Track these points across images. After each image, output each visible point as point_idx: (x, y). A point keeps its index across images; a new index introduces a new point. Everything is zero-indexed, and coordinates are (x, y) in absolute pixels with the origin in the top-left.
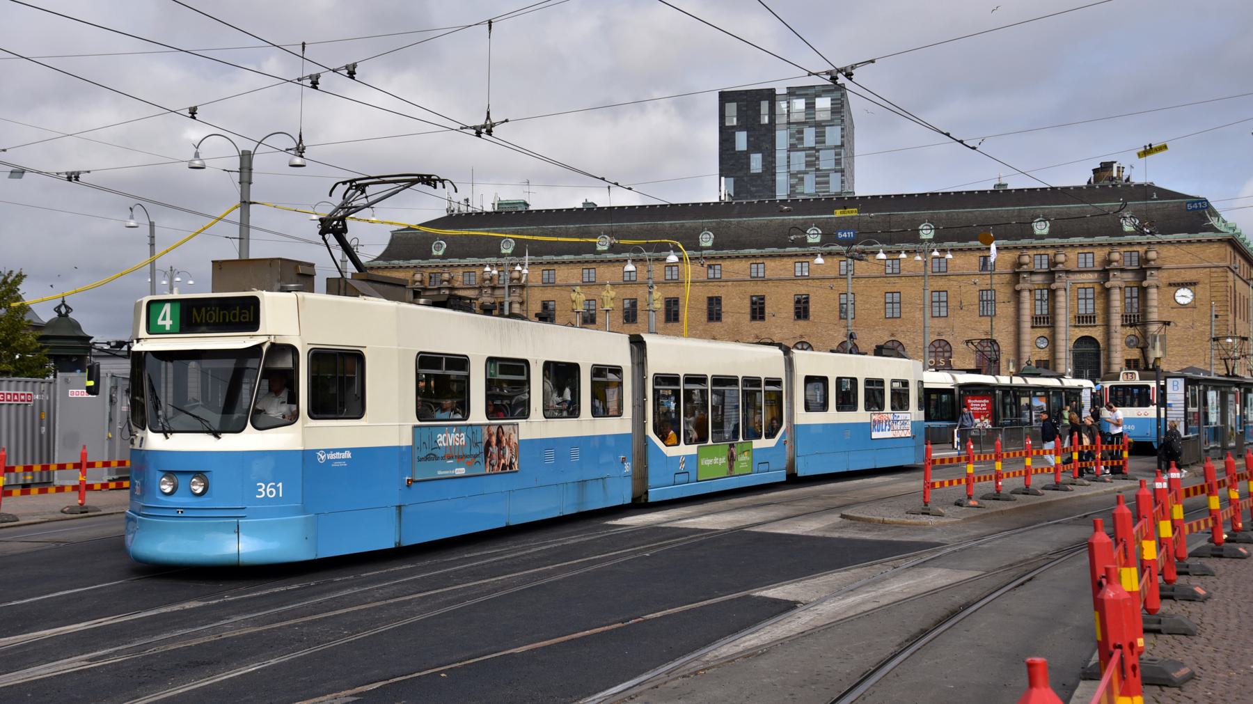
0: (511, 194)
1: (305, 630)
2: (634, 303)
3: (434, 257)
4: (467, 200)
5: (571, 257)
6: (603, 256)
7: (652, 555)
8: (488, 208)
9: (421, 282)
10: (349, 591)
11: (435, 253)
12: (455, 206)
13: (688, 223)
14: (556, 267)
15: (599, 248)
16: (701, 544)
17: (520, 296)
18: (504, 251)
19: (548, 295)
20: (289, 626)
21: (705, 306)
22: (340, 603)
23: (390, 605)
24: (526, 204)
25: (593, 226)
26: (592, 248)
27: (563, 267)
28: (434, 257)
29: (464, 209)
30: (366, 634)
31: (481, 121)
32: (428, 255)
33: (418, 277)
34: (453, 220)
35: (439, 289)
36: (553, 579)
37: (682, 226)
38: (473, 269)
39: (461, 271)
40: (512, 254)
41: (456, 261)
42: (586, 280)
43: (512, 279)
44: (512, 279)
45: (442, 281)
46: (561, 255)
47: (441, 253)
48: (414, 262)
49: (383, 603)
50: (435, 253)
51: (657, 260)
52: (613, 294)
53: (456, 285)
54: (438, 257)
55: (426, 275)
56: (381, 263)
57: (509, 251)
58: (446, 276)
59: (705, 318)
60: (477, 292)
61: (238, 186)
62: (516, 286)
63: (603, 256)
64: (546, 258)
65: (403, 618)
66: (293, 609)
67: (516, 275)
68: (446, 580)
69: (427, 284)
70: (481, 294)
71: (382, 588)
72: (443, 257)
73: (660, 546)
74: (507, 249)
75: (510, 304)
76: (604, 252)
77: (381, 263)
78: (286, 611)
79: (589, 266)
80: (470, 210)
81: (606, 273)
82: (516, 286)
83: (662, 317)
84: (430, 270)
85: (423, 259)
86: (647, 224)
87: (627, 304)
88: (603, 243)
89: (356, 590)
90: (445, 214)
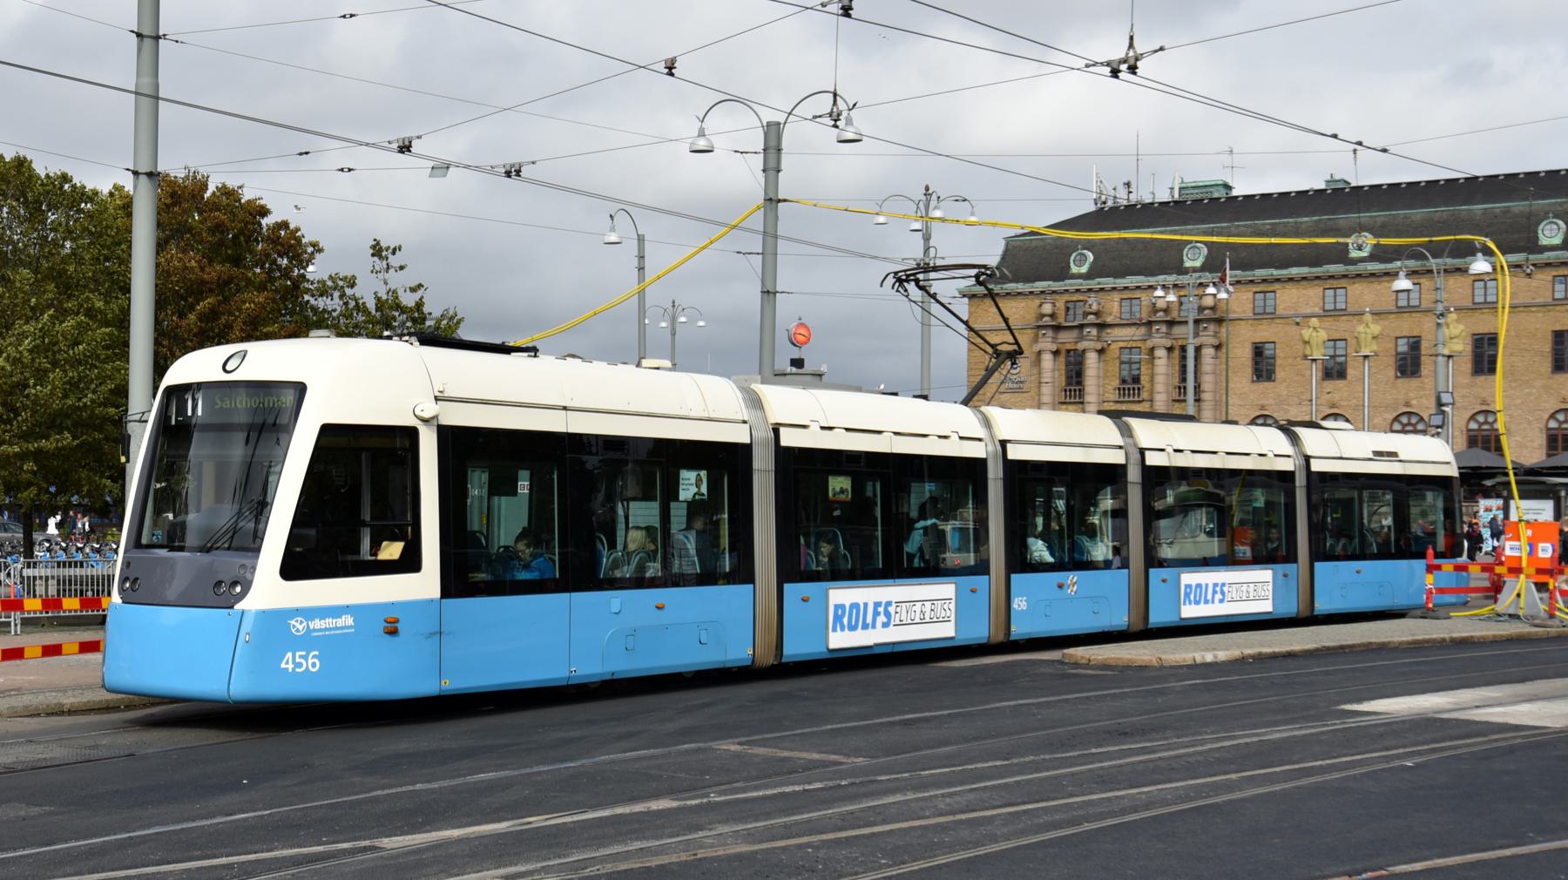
0: (1203, 172)
1: (822, 854)
2: (1415, 345)
3: (1074, 277)
4: (1128, 184)
5: (1304, 270)
6: (1361, 267)
7: (1417, 766)
8: (1163, 196)
9: (1052, 316)
10: (899, 798)
11: (1074, 269)
13: (1517, 206)
14: (1276, 286)
15: (1354, 254)
16: (1512, 750)
17: (1216, 335)
19: (1264, 333)
20: (799, 846)
21: (1547, 347)
22: (881, 815)
23: (961, 822)
24: (1228, 187)
25: (1343, 219)
26: (1341, 255)
27: (1289, 285)
28: (1074, 277)
30: (916, 866)
31: (1118, 51)
32: (1063, 274)
33: (1047, 308)
34: (1104, 217)
35: (1081, 326)
36: (1238, 795)
37: (1506, 211)
38: (1137, 294)
39: (1116, 297)
40: (1203, 269)
41: (1108, 282)
42: (1329, 306)
43: (1201, 309)
44: (1201, 309)
45: (1086, 314)
46: (1286, 267)
47: (1084, 269)
48: (1040, 285)
49: (951, 818)
50: (1074, 269)
51: (1458, 270)
52: (1375, 329)
53: (1109, 320)
54: (1080, 276)
55: (1061, 305)
57: (1198, 264)
59: (1547, 365)
60: (1143, 330)
61: (761, 177)
62: (1209, 320)
63: (1361, 267)
64: (1260, 273)
65: (977, 844)
66: (809, 821)
67: (1208, 301)
68: (1055, 788)
69: (1061, 320)
70: (1150, 335)
71: (951, 795)
72: (1088, 276)
73: (1434, 750)
74: (1194, 260)
75: (1198, 349)
76: (1363, 260)
78: (797, 823)
79: (1335, 283)
80: (1133, 198)
81: (1362, 294)
82: (1209, 320)
83: (1467, 366)
84: (1067, 297)
85: (1055, 280)
86: (1441, 211)
87: (1403, 347)
88: (1362, 244)
89: (910, 796)
90: (1092, 208)
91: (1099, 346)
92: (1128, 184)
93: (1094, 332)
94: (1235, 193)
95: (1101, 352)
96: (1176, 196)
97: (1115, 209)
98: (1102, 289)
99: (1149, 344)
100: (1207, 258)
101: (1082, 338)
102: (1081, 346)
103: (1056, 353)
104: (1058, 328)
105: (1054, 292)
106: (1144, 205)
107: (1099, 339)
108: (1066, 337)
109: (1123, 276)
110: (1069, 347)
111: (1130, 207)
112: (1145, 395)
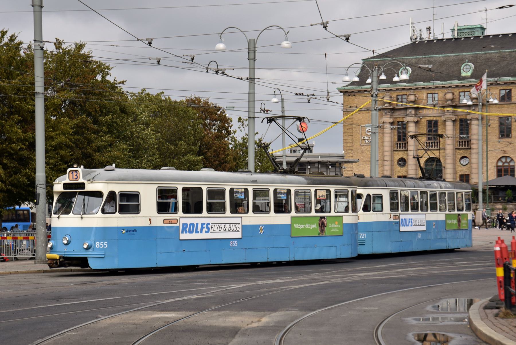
4: (429, 29)
8: (449, 36)
24: (483, 29)
29: (425, 36)
34: (417, 47)
35: (406, 109)
38: (436, 91)
40: (472, 77)
41: (420, 84)
55: (394, 95)
56: (355, 88)
58: (412, 98)
74: (467, 70)
77: (355, 88)
84: (398, 93)
90: (409, 42)
93: (413, 112)
94: (486, 33)
95: (417, 123)
96: (456, 36)
97: (422, 43)
98: (417, 89)
101: (407, 115)
102: (406, 120)
104: (393, 110)
107: (416, 115)
108: (399, 116)
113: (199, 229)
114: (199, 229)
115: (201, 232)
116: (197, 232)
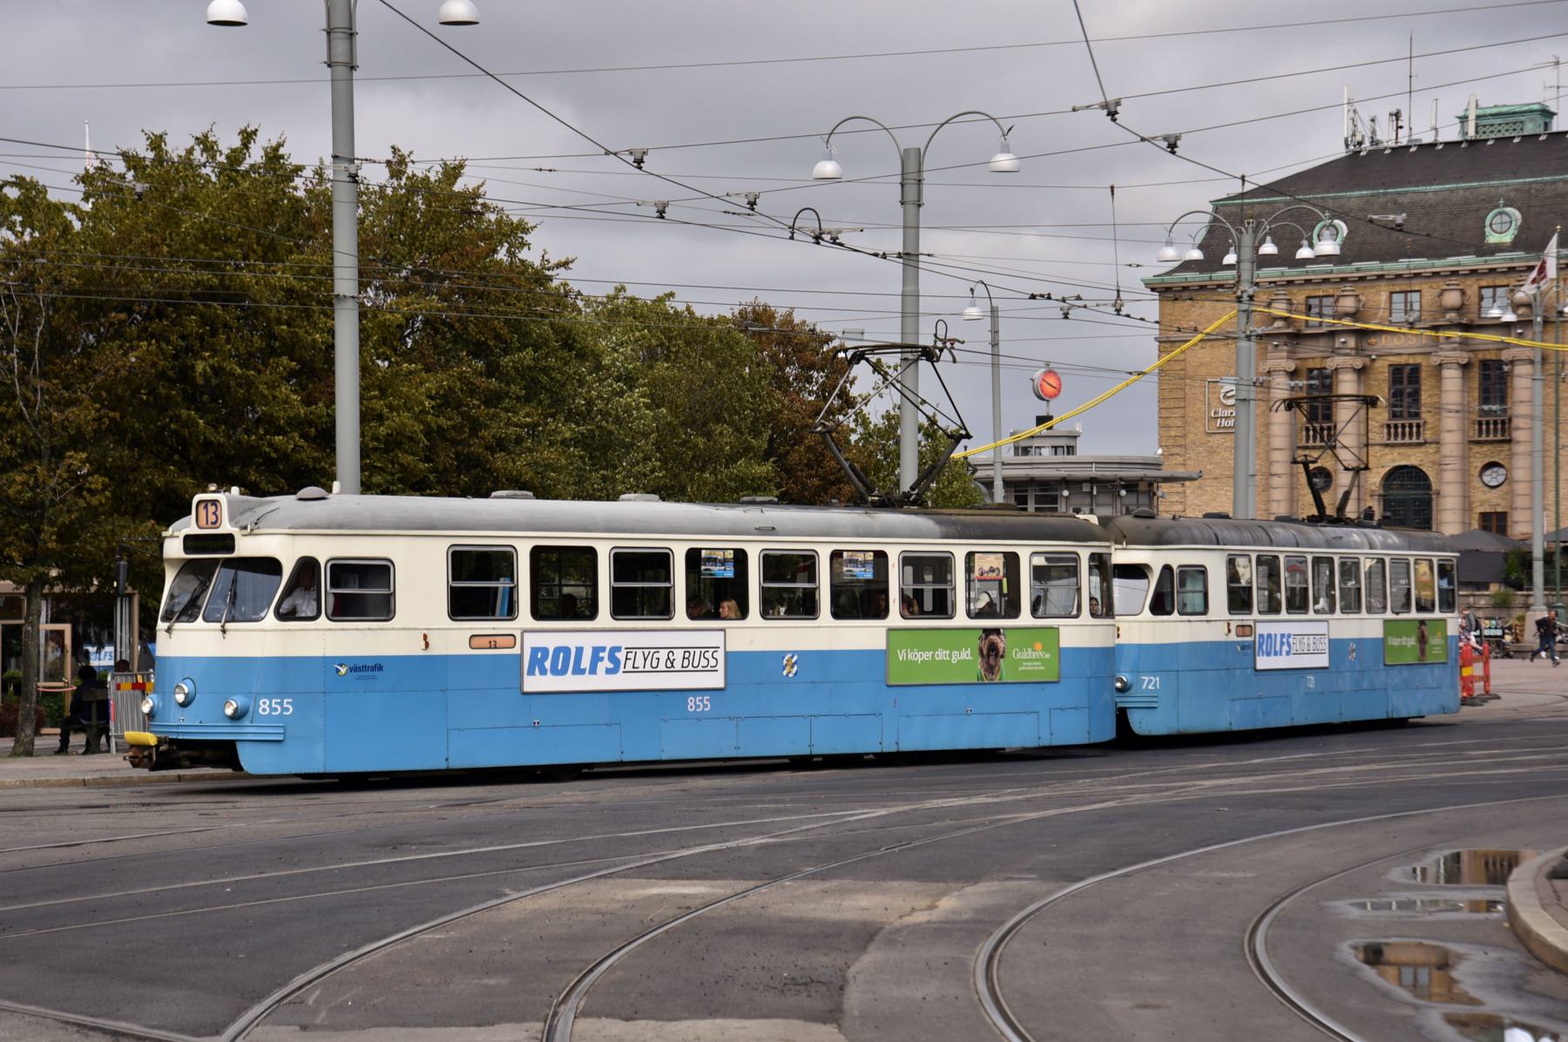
4: (1397, 115)
8: (1451, 134)
12: (1364, 131)
18: (1493, 238)
24: (1547, 114)
29: (1387, 136)
34: (1363, 166)
35: (1332, 334)
40: (1515, 245)
41: (1372, 267)
56: (1193, 277)
57: (1507, 238)
58: (1348, 304)
74: (1502, 229)
90: (1339, 152)
91: (1359, 363)
92: (1397, 115)
93: (1352, 342)
95: (1361, 372)
96: (1471, 133)
97: (1377, 154)
98: (1362, 279)
99: (1435, 360)
100: (1521, 229)
101: (1335, 352)
102: (1332, 363)
103: (1293, 375)
104: (1296, 337)
105: (1290, 283)
106: (1421, 146)
107: (1359, 351)
109: (1395, 258)
110: (1311, 364)
111: (1399, 151)
112: (1427, 435)
113: (586, 662)
114: (586, 662)
115: (593, 671)
116: (578, 671)
